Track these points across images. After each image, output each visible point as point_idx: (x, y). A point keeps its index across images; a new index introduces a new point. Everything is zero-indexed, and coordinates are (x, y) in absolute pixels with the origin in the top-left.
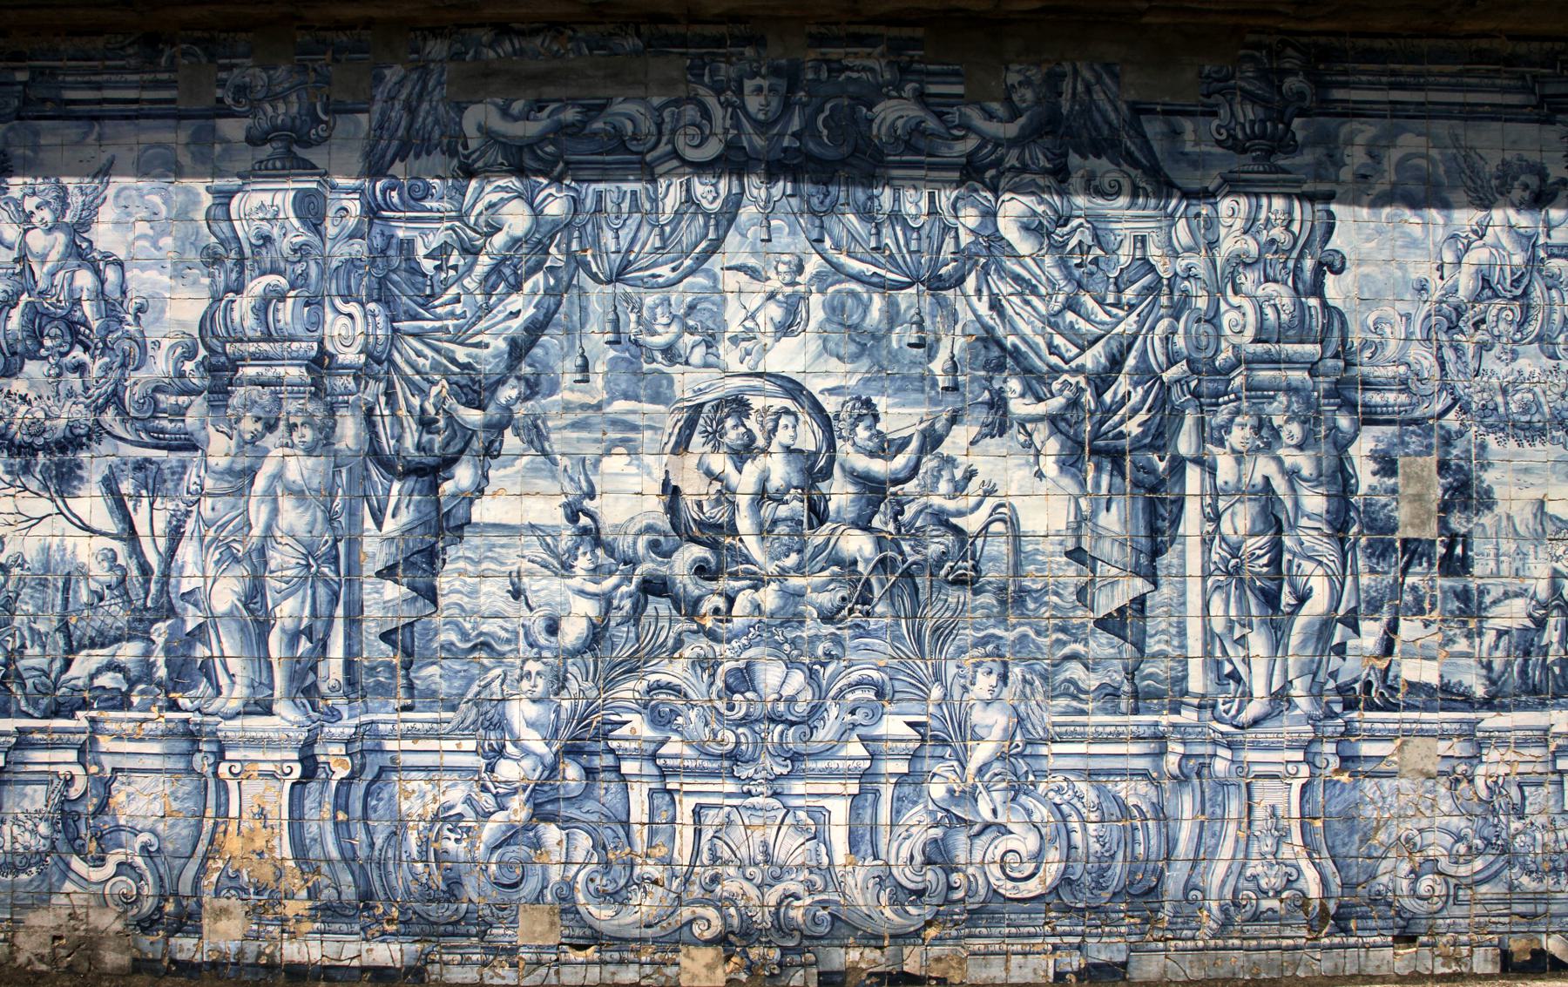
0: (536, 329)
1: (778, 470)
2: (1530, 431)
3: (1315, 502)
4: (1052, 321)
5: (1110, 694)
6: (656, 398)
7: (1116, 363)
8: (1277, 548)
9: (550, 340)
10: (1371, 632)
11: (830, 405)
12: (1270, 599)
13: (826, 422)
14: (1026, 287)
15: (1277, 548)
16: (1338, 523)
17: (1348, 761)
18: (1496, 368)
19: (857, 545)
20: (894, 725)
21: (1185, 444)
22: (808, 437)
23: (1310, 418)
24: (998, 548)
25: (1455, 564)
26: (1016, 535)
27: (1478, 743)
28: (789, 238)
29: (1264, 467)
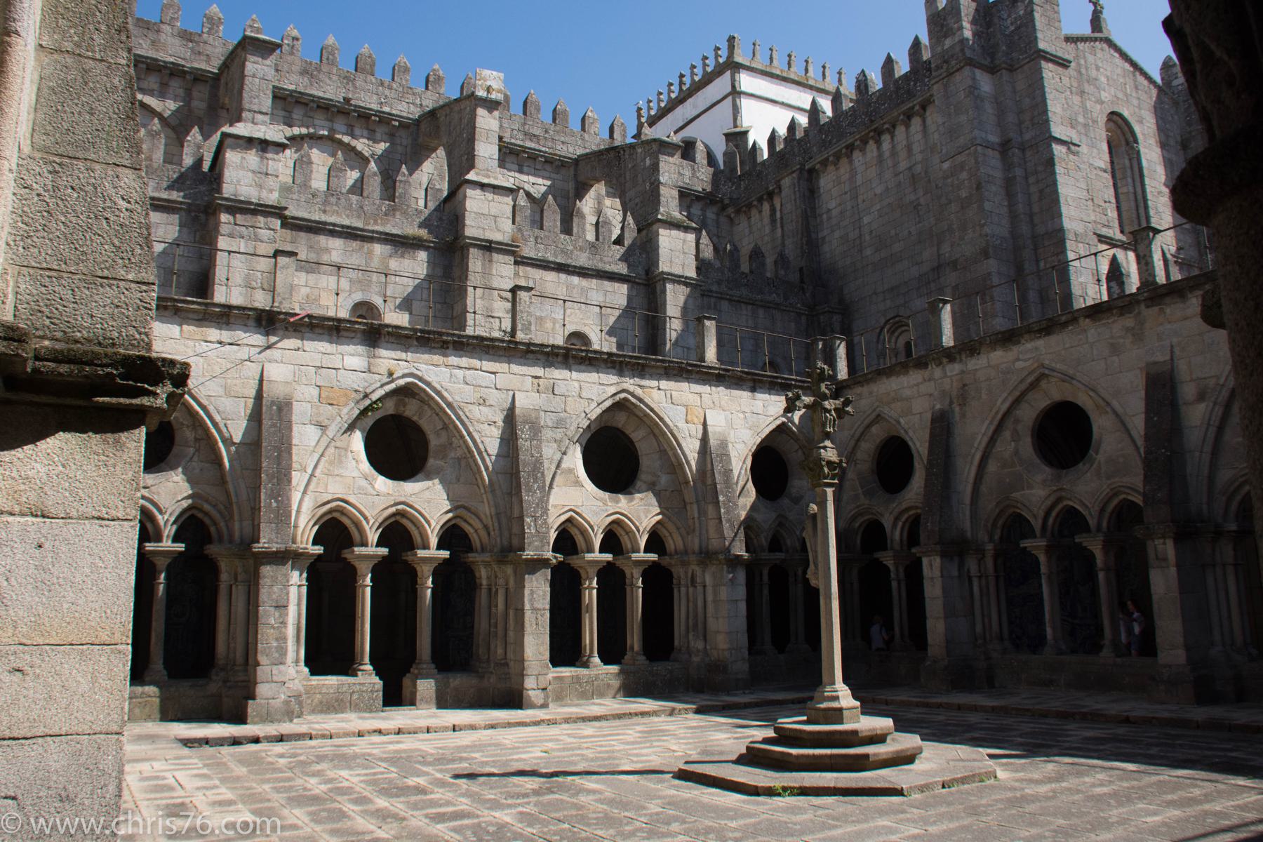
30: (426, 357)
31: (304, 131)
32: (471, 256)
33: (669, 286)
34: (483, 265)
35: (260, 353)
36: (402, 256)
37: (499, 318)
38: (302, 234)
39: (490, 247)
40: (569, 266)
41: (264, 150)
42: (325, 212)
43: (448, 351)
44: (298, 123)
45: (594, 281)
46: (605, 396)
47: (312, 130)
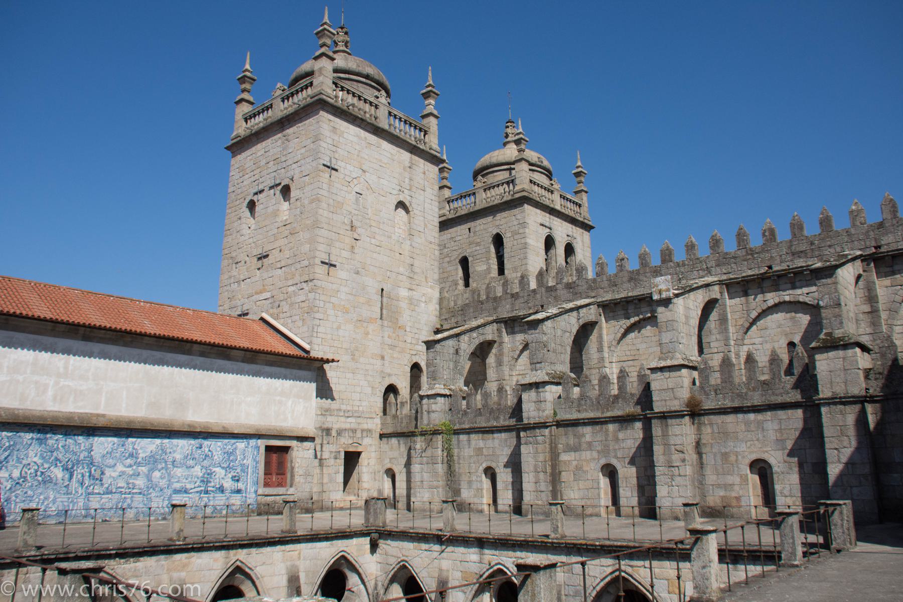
0: (8, 456)
1: (32, 471)
2: (110, 467)
3: (88, 474)
4: (63, 456)
5: (64, 494)
6: (21, 463)
7: (69, 460)
8: (83, 479)
9: (9, 457)
10: (92, 487)
11: (39, 464)
12: (82, 484)
13: (38, 466)
14: (61, 453)
15: (83, 479)
16: (90, 476)
17: (88, 500)
18: (107, 461)
19: (40, 479)
20: (42, 497)
21: (75, 468)
22: (36, 468)
23: (88, 465)
24: (55, 479)
25: (101, 480)
26: (56, 478)
27: (102, 498)
28: (37, 447)
29: (82, 471)
30: (505, 552)
31: (637, 319)
32: (653, 425)
33: (824, 410)
34: (662, 430)
35: (440, 554)
36: (626, 429)
37: (677, 466)
38: (570, 429)
39: (664, 415)
40: (742, 407)
41: (537, 388)
42: (579, 411)
43: (516, 549)
44: (632, 314)
45: (769, 413)
46: (605, 574)
47: (641, 317)
